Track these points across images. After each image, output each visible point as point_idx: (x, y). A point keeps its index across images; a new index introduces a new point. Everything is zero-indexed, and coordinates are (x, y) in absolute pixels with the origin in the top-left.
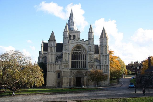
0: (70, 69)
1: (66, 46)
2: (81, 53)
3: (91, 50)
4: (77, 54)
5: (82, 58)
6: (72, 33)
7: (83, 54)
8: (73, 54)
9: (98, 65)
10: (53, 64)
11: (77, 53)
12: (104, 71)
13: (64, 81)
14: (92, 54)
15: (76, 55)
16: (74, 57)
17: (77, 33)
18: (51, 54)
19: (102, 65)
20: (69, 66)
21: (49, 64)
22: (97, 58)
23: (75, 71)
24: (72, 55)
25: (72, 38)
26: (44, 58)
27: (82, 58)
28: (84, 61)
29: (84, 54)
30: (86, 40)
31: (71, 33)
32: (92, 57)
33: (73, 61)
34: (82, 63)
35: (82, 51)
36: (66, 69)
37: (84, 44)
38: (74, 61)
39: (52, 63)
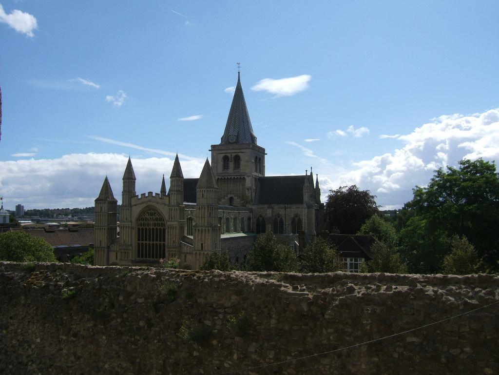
1: (125, 211)
2: (155, 225)
5: (157, 236)
6: (231, 151)
11: (148, 225)
16: (142, 234)
17: (244, 151)
18: (99, 228)
19: (194, 252)
24: (139, 229)
25: (231, 165)
28: (162, 242)
31: (230, 151)
33: (141, 242)
35: (157, 219)
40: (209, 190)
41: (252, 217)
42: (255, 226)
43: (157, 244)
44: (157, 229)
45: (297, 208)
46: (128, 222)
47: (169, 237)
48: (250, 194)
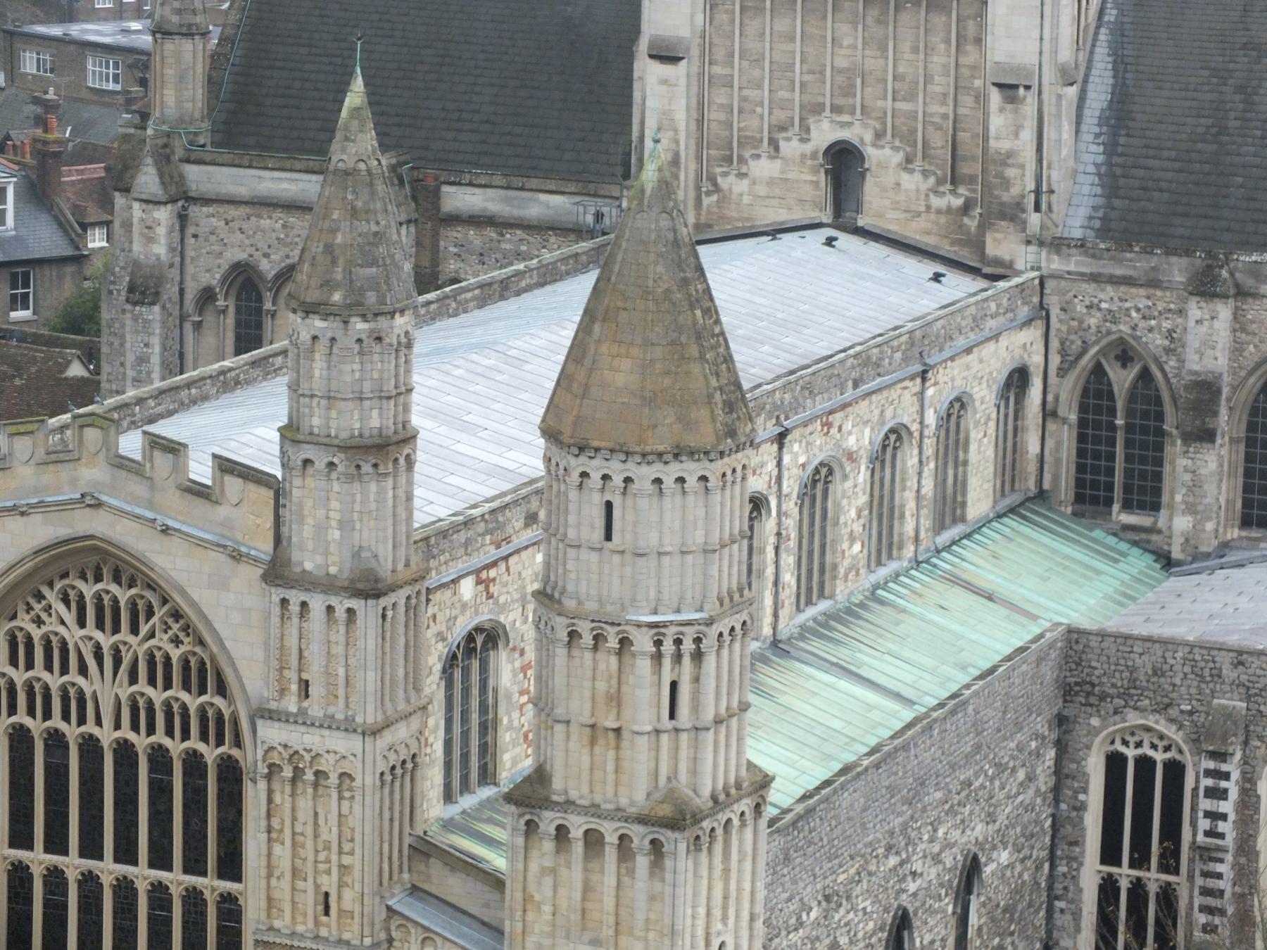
2: (141, 715)
4: (72, 732)
11: (76, 704)
26: (207, 296)
28: (211, 885)
30: (225, 466)
32: (327, 847)
35: (160, 671)
37: (176, 541)
40: (670, 473)
41: (1037, 360)
42: (1065, 439)
43: (159, 894)
44: (160, 758)
47: (282, 853)
48: (1028, 135)
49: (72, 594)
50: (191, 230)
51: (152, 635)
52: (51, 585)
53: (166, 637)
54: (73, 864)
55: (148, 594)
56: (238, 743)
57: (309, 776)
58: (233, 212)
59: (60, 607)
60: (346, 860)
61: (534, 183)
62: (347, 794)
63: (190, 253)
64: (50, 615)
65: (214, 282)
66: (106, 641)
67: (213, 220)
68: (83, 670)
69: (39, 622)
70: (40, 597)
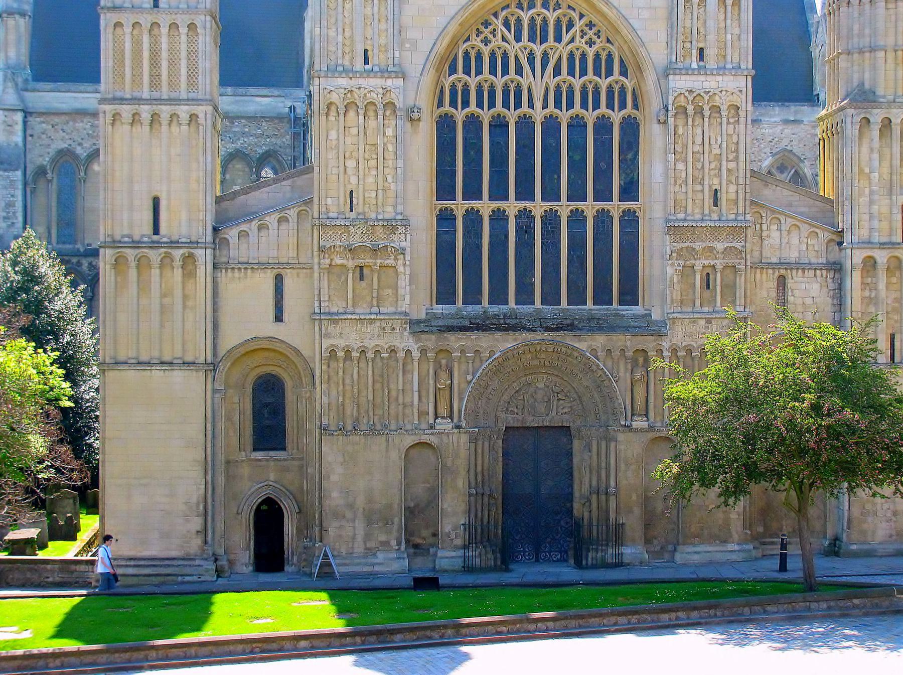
0: (418, 327)
3: (710, 53)
4: (512, 117)
5: (578, 167)
7: (590, 117)
8: (460, 116)
9: (800, 266)
10: (189, 259)
12: (883, 344)
13: (335, 494)
14: (716, 109)
15: (499, 125)
18: (145, 111)
19: (859, 256)
20: (403, 282)
21: (119, 263)
22: (782, 169)
23: (484, 341)
24: (445, 125)
26: (41, 172)
27: (578, 167)
28: (616, 207)
29: (616, 117)
33: (459, 206)
34: (577, 245)
36: (375, 328)
38: (473, 218)
39: (174, 244)
45: (786, 122)
46: (384, 73)
49: (512, 20)
50: (29, 132)
51: (572, 40)
52: (495, 15)
53: (583, 41)
54: (512, 207)
55: (572, 12)
56: (636, 106)
57: (706, 108)
58: (56, 120)
59: (504, 29)
60: (732, 165)
61: (252, 90)
62: (731, 120)
63: (28, 146)
64: (494, 36)
65: (45, 163)
66: (538, 50)
67: (44, 125)
68: (519, 71)
69: (486, 42)
70: (486, 24)
